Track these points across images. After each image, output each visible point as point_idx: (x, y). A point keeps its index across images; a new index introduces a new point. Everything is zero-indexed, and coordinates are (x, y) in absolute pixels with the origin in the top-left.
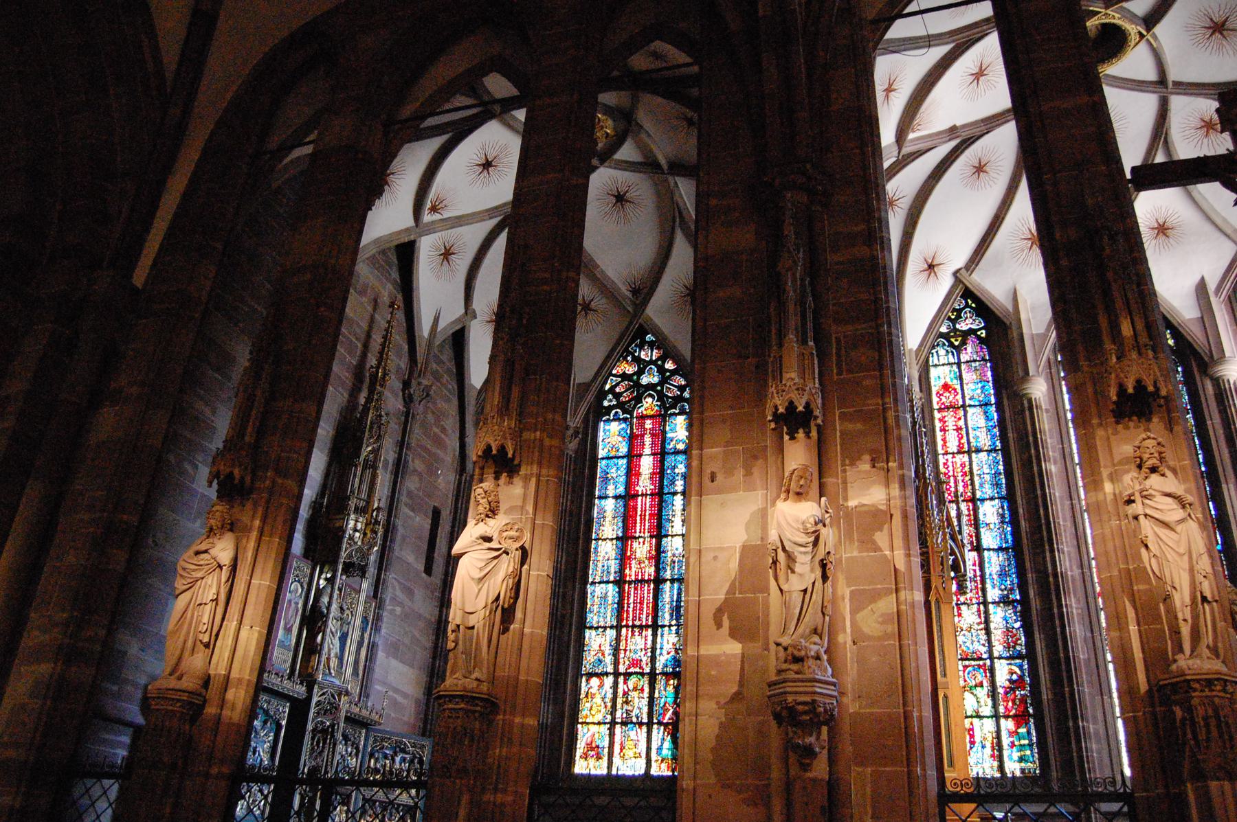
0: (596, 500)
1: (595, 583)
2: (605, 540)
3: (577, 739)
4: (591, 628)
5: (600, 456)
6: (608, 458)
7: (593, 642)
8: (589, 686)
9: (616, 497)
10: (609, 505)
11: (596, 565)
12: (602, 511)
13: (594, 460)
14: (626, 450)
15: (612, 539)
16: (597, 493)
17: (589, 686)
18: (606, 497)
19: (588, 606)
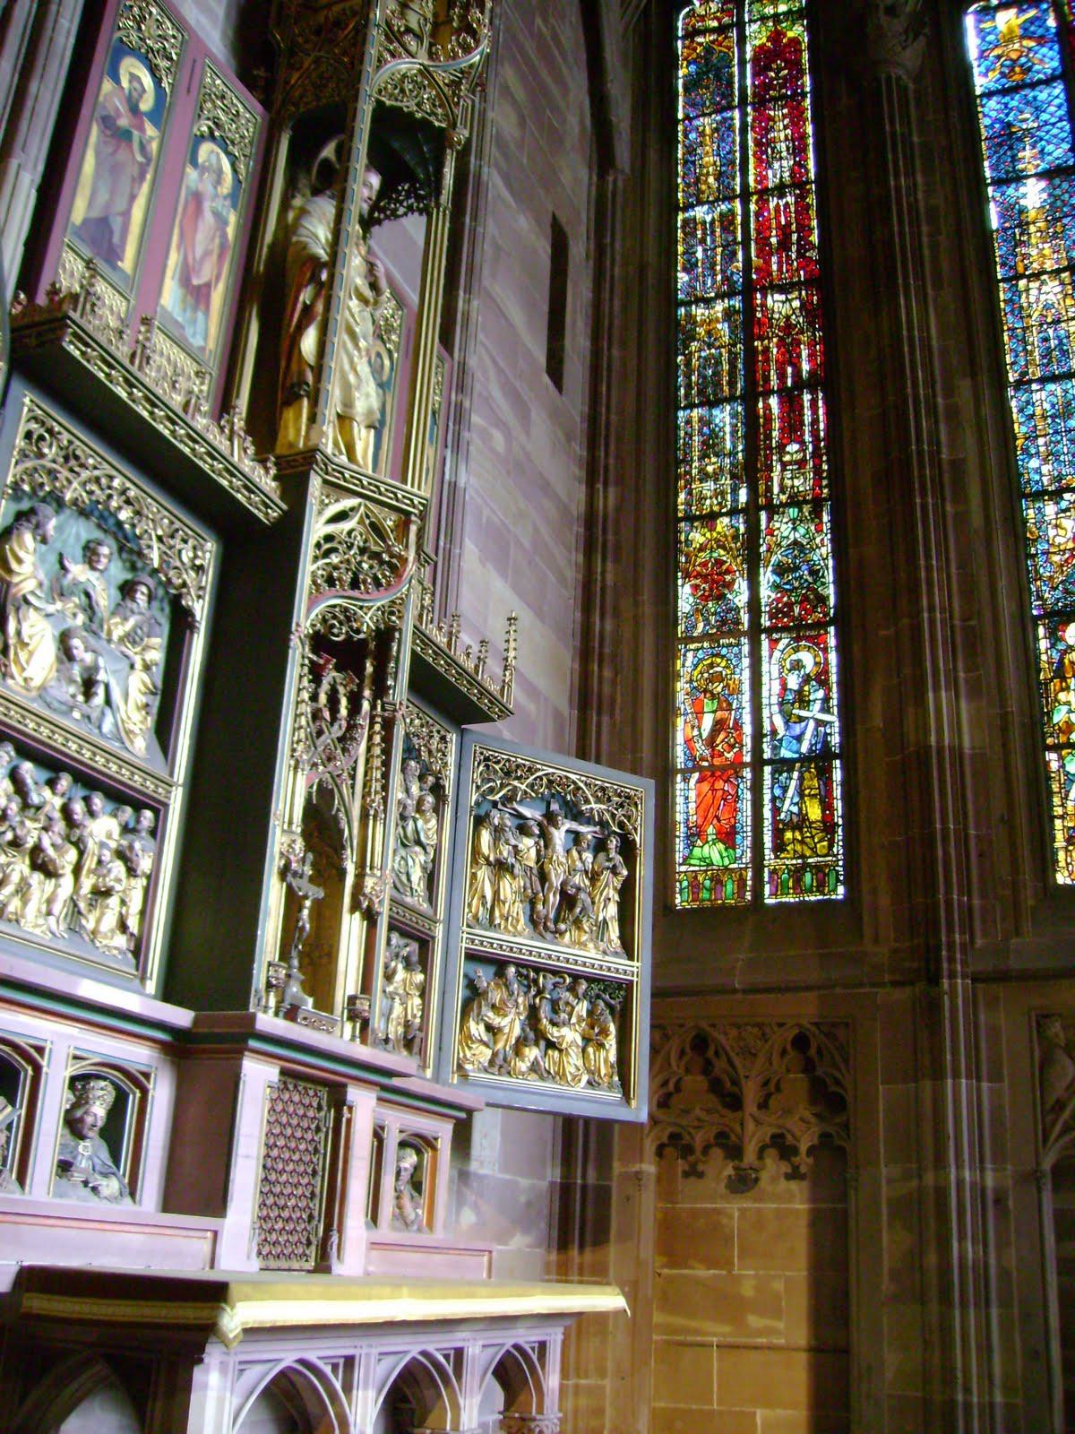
0: (990, 189)
1: (1030, 382)
2: (1036, 276)
3: (1050, 794)
4: (1040, 495)
5: (978, 91)
6: (1004, 92)
7: (1052, 532)
8: (1061, 646)
9: (1046, 175)
10: (1033, 195)
11: (1024, 341)
12: (1015, 214)
13: (967, 103)
14: (1055, 64)
15: (1057, 272)
16: (988, 174)
17: (1061, 646)
18: (1018, 178)
19: (1019, 442)
